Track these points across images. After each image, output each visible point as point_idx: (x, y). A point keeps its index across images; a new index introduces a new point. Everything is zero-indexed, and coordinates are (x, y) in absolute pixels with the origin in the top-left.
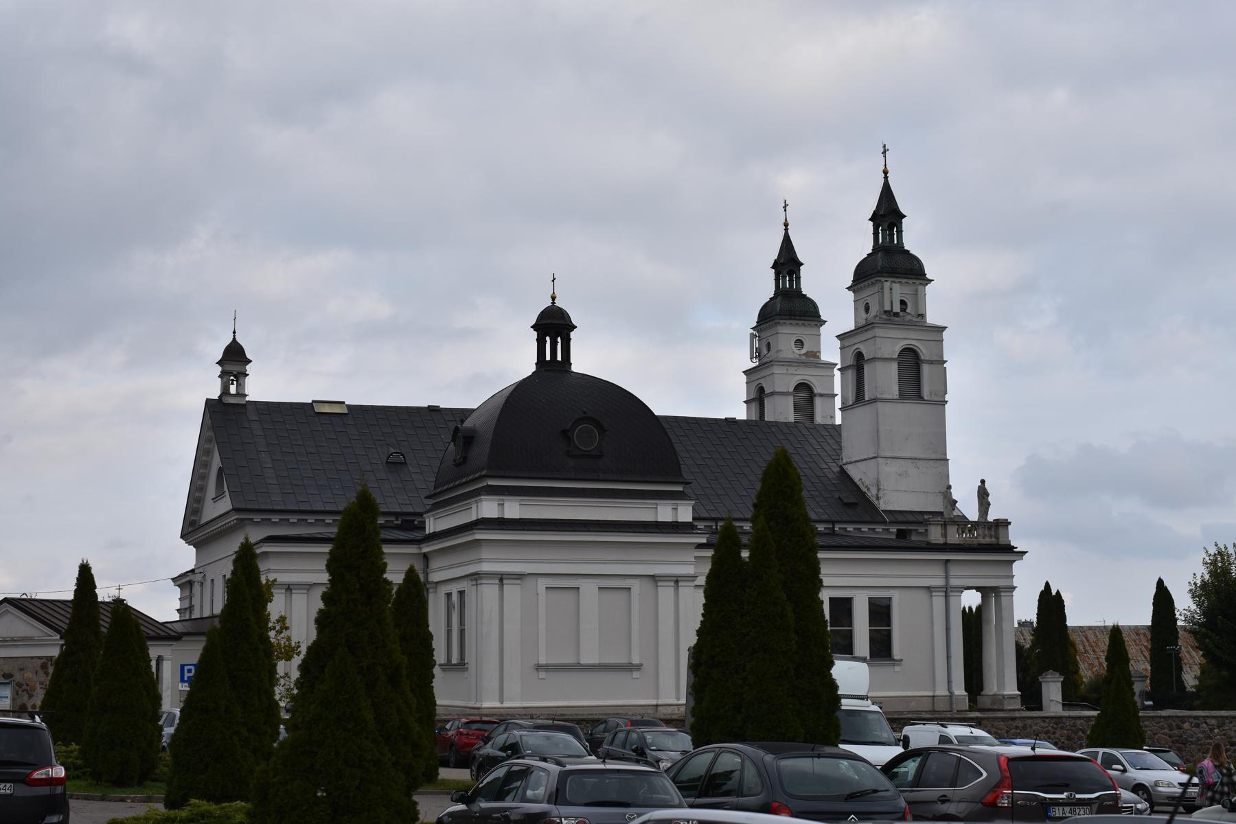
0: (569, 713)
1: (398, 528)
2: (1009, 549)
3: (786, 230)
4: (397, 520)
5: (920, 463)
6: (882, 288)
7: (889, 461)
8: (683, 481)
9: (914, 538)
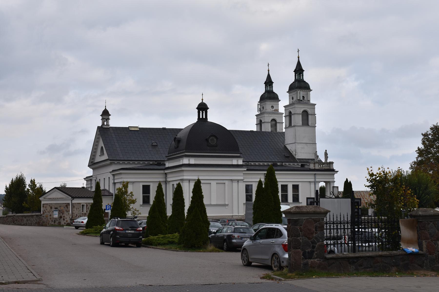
0: (210, 218)
1: (156, 165)
2: (333, 170)
3: (269, 72)
4: (156, 163)
5: (308, 145)
6: (297, 93)
7: (299, 144)
8: (240, 153)
9: (306, 167)
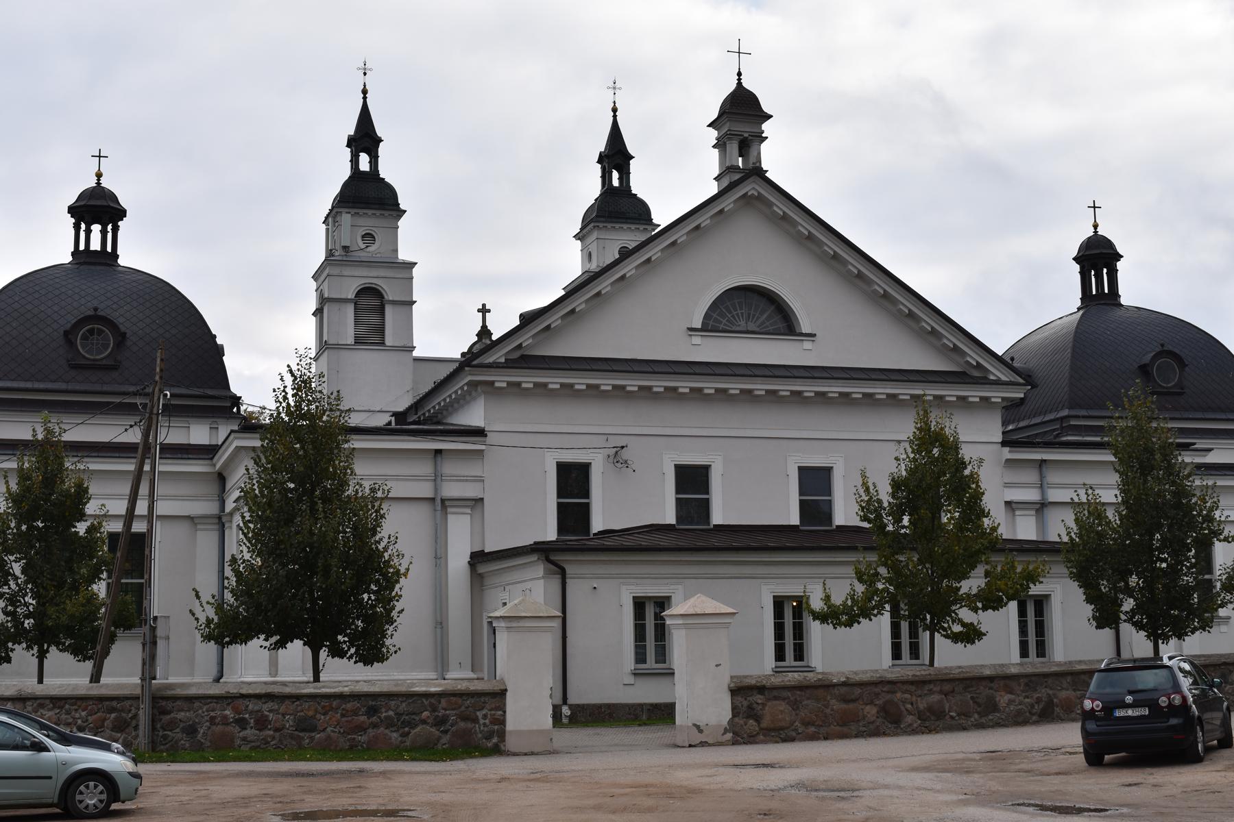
3: (365, 98)
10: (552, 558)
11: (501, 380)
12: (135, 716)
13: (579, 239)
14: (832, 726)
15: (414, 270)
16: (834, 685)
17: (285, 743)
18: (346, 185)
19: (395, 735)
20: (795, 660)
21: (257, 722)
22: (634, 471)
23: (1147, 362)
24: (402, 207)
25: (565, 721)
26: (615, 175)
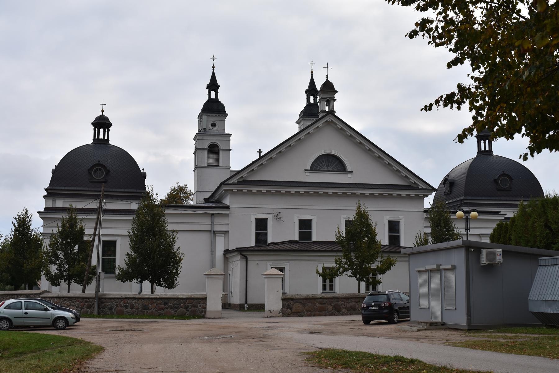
3: (213, 70)
10: (243, 253)
11: (235, 189)
12: (94, 304)
13: (298, 123)
14: (317, 312)
15: (231, 137)
16: (317, 299)
17: (139, 313)
18: (205, 105)
19: (173, 311)
20: (330, 290)
21: (131, 306)
22: (283, 221)
23: (497, 178)
24: (227, 112)
25: (246, 309)
26: (312, 98)
